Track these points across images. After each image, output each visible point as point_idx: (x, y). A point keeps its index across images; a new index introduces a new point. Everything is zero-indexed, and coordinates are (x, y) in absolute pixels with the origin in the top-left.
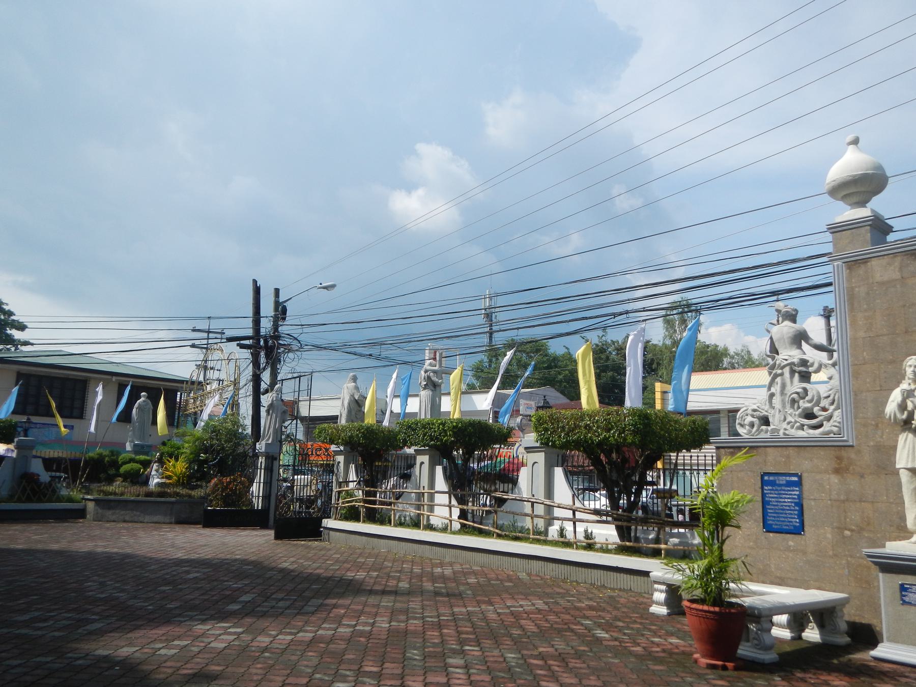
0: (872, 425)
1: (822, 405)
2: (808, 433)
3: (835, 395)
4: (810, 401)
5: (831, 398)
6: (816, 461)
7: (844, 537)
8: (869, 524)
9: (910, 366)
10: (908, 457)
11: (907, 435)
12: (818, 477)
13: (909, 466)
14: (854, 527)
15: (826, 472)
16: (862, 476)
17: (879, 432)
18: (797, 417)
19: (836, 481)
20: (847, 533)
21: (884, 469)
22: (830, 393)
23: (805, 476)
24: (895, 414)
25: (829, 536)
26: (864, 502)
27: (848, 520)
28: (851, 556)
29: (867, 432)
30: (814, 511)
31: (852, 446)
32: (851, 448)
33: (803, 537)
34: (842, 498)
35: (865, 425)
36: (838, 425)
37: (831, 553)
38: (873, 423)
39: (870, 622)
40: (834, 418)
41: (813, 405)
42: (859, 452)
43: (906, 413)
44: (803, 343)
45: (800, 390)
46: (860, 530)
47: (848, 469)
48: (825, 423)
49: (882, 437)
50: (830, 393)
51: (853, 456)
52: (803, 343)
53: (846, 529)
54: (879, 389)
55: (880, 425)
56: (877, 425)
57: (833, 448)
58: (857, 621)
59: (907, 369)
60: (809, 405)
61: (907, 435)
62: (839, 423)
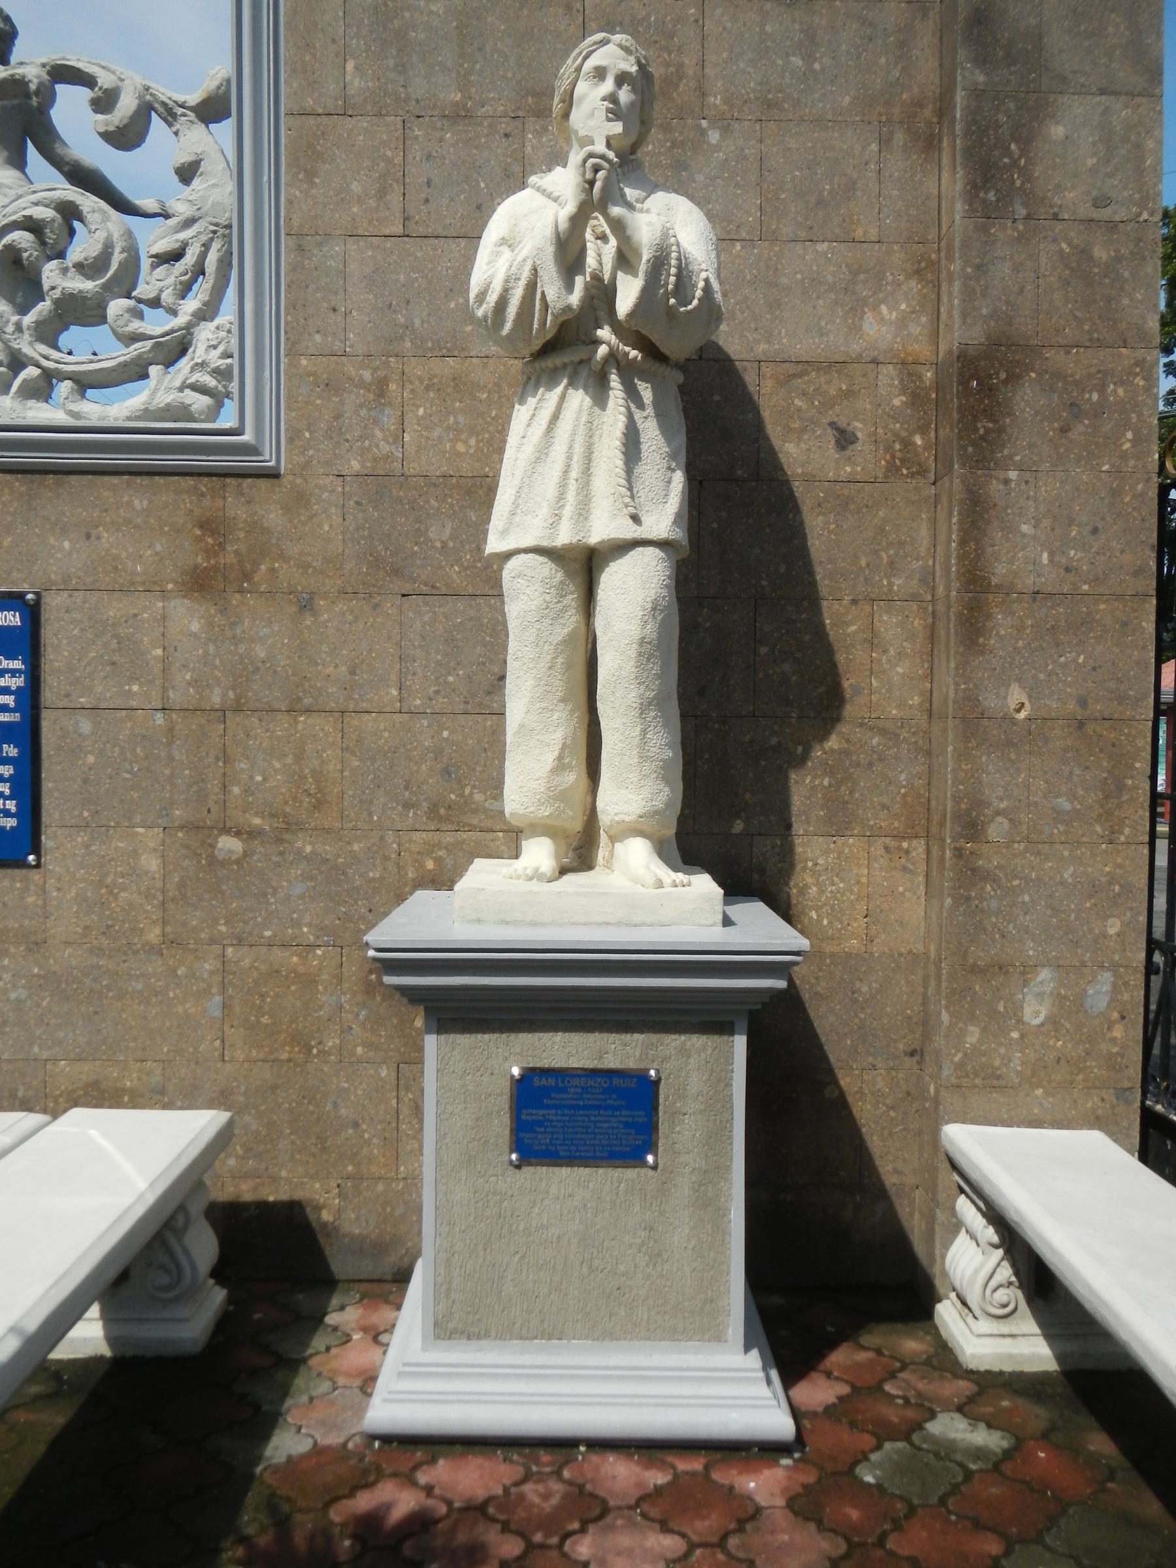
0: (362, 384)
1: (143, 290)
2: (71, 414)
3: (206, 246)
4: (86, 269)
5: (190, 258)
6: (107, 538)
7: (213, 861)
8: (318, 805)
9: (600, 73)
10: (561, 497)
11: (563, 397)
12: (115, 608)
13: (564, 537)
14: (257, 821)
15: (153, 587)
16: (306, 606)
17: (389, 419)
18: (27, 336)
19: (195, 627)
20: (229, 845)
21: (397, 572)
22: (184, 235)
23: (53, 604)
24: (532, 286)
25: (151, 863)
26: (308, 711)
27: (236, 790)
28: (239, 942)
29: (337, 417)
30: (91, 759)
31: (273, 475)
32: (263, 484)
33: (35, 875)
34: (216, 699)
35: (331, 386)
36: (211, 382)
37: (153, 935)
38: (367, 375)
39: (298, 1195)
40: (199, 351)
41: (106, 287)
42: (301, 498)
43: (579, 282)
44: (32, 152)
45: (45, 213)
46: (288, 826)
47: (247, 577)
48: (154, 370)
49: (398, 438)
50: (184, 235)
51: (273, 517)
52: (32, 152)
53: (226, 831)
54: (399, 230)
55: (392, 386)
56: (380, 388)
57: (190, 481)
58: (248, 1197)
59: (582, 87)
60: (88, 286)
61: (563, 397)
62: (222, 374)
